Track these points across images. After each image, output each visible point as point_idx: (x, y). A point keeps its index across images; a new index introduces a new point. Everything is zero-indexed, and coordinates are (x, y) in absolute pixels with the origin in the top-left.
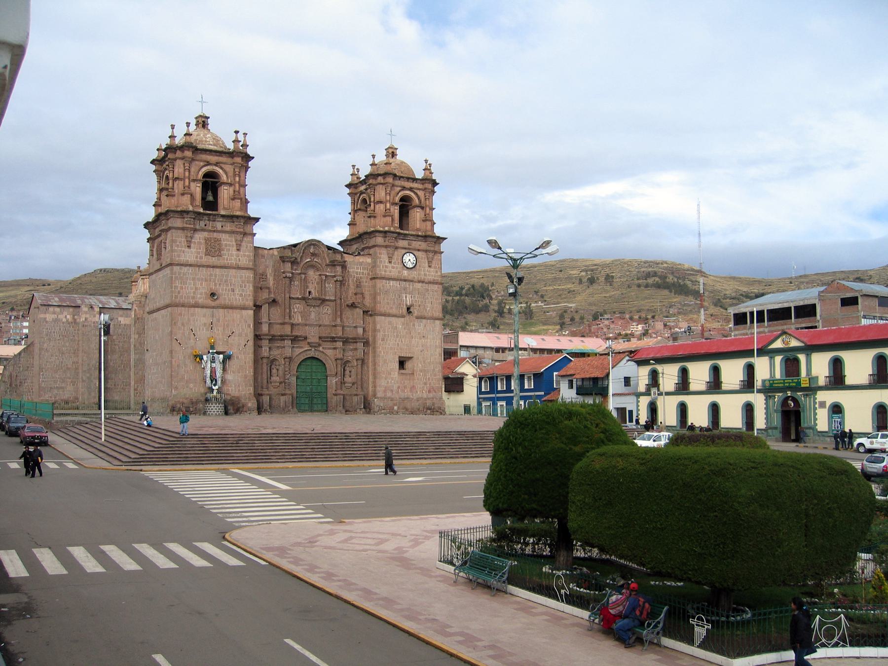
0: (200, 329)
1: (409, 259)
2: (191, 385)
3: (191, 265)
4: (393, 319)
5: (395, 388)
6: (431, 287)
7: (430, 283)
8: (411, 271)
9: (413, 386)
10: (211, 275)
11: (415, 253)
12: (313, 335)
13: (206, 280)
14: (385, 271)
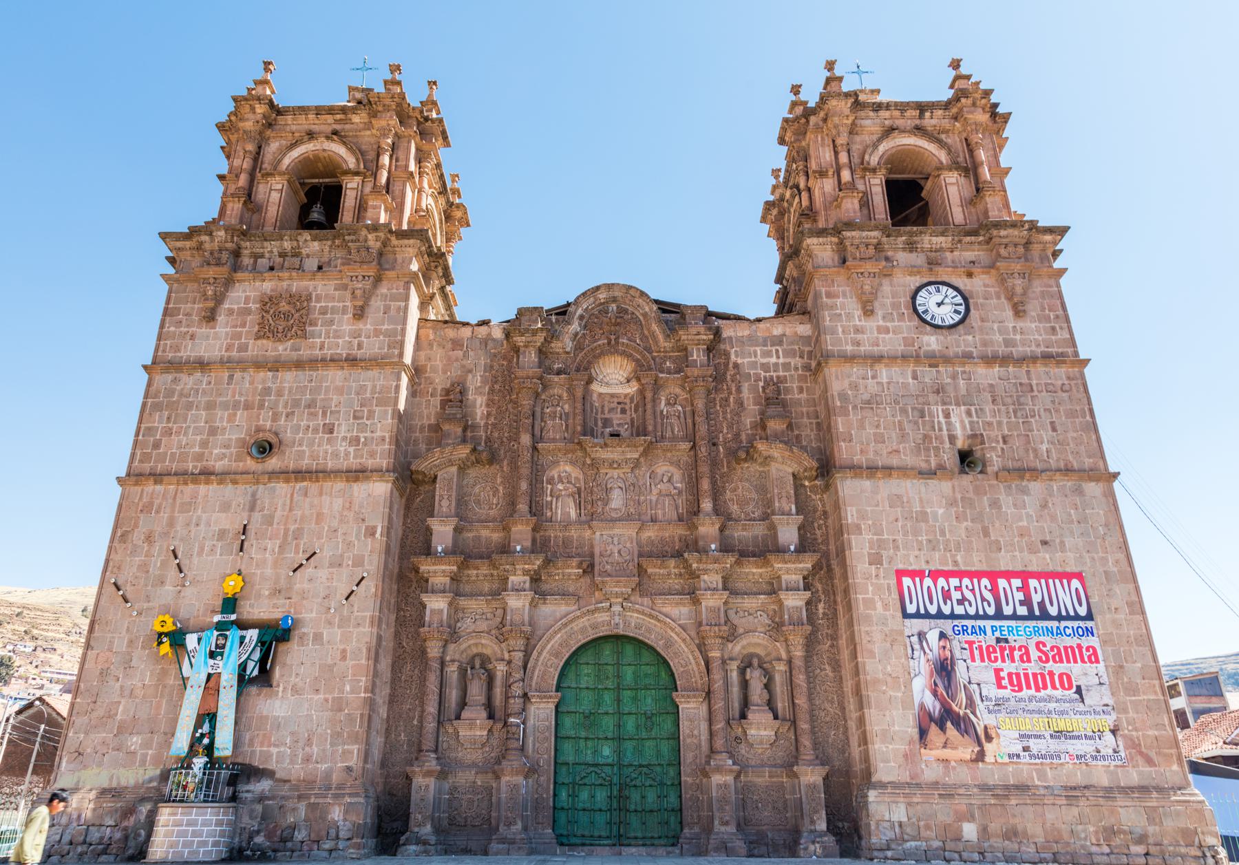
0: (202, 549)
2: (134, 742)
4: (910, 488)
8: (951, 338)
10: (267, 391)
13: (247, 406)
14: (858, 344)
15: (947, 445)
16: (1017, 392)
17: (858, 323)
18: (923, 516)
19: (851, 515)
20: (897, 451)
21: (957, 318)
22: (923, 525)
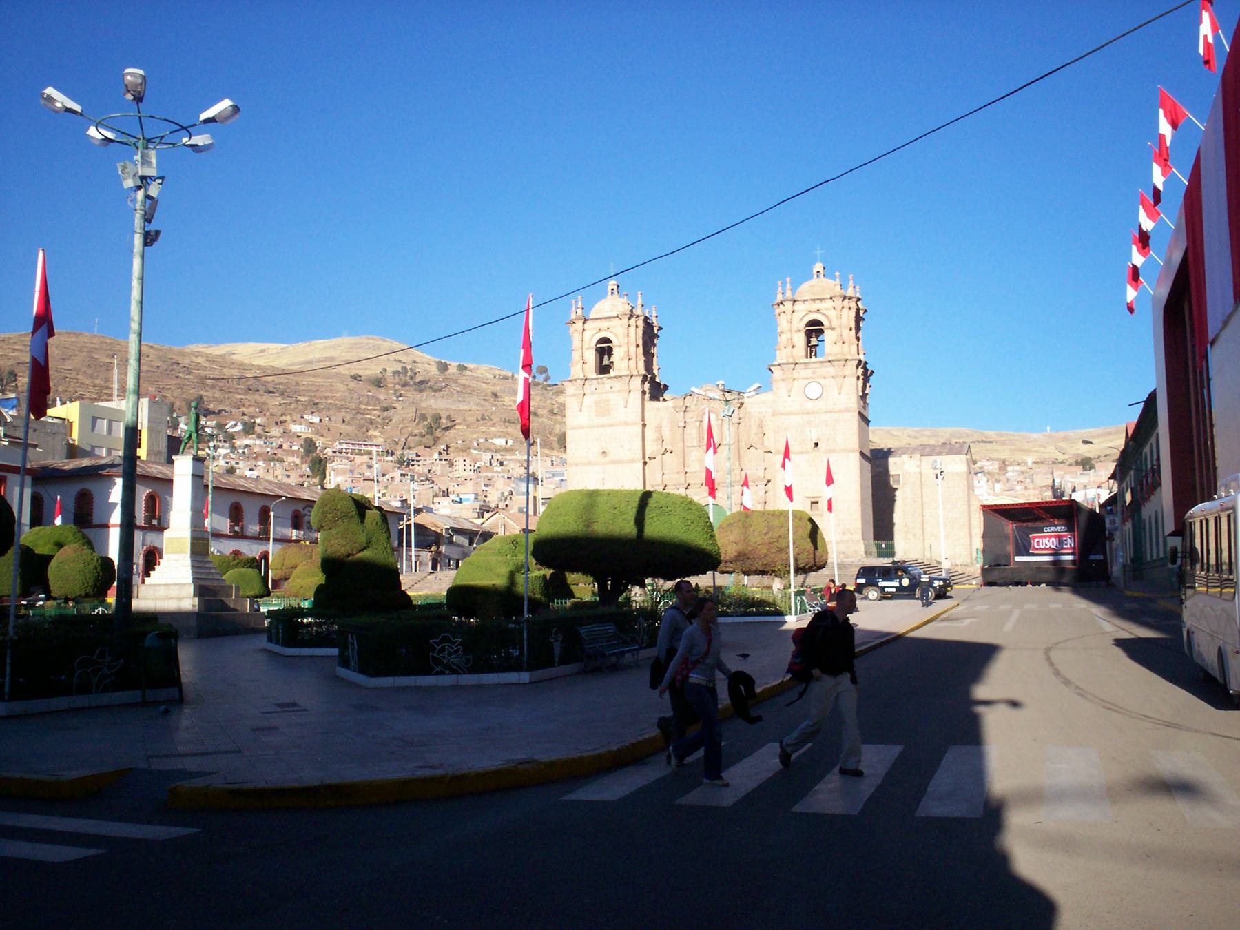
1: (814, 391)
3: (582, 428)
7: (840, 411)
11: (822, 381)
14: (784, 407)
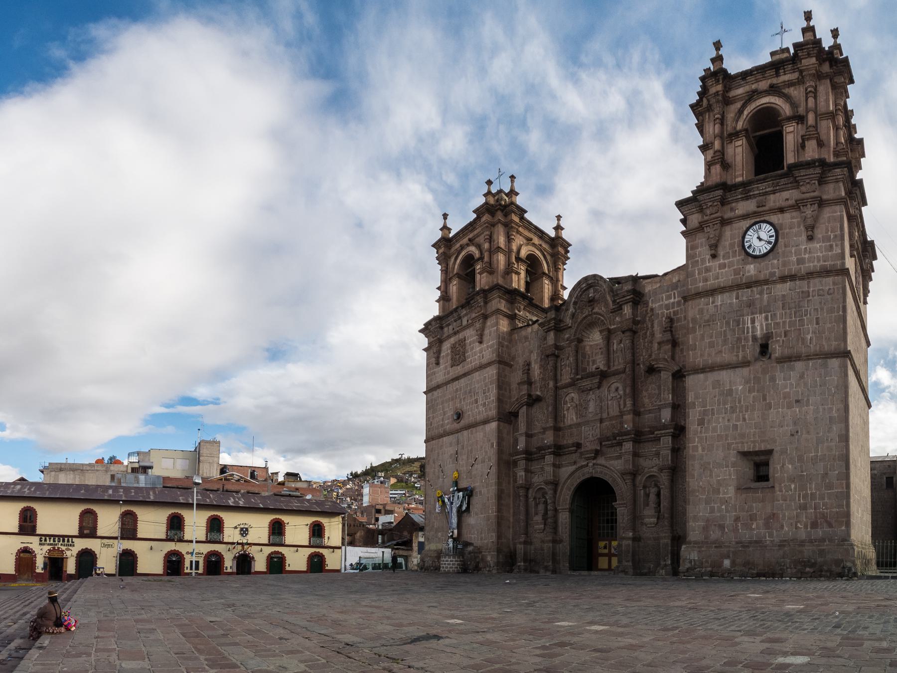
4: (724, 375)
5: (729, 522)
6: (816, 284)
7: (810, 275)
8: (764, 263)
9: (774, 516)
12: (589, 436)
15: (751, 343)
16: (799, 298)
17: (708, 265)
18: (730, 392)
19: (690, 397)
20: (721, 352)
21: (769, 247)
22: (729, 398)
